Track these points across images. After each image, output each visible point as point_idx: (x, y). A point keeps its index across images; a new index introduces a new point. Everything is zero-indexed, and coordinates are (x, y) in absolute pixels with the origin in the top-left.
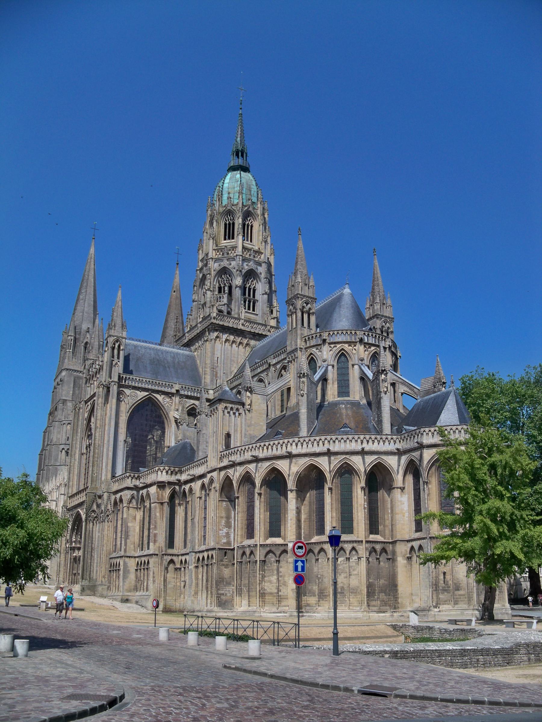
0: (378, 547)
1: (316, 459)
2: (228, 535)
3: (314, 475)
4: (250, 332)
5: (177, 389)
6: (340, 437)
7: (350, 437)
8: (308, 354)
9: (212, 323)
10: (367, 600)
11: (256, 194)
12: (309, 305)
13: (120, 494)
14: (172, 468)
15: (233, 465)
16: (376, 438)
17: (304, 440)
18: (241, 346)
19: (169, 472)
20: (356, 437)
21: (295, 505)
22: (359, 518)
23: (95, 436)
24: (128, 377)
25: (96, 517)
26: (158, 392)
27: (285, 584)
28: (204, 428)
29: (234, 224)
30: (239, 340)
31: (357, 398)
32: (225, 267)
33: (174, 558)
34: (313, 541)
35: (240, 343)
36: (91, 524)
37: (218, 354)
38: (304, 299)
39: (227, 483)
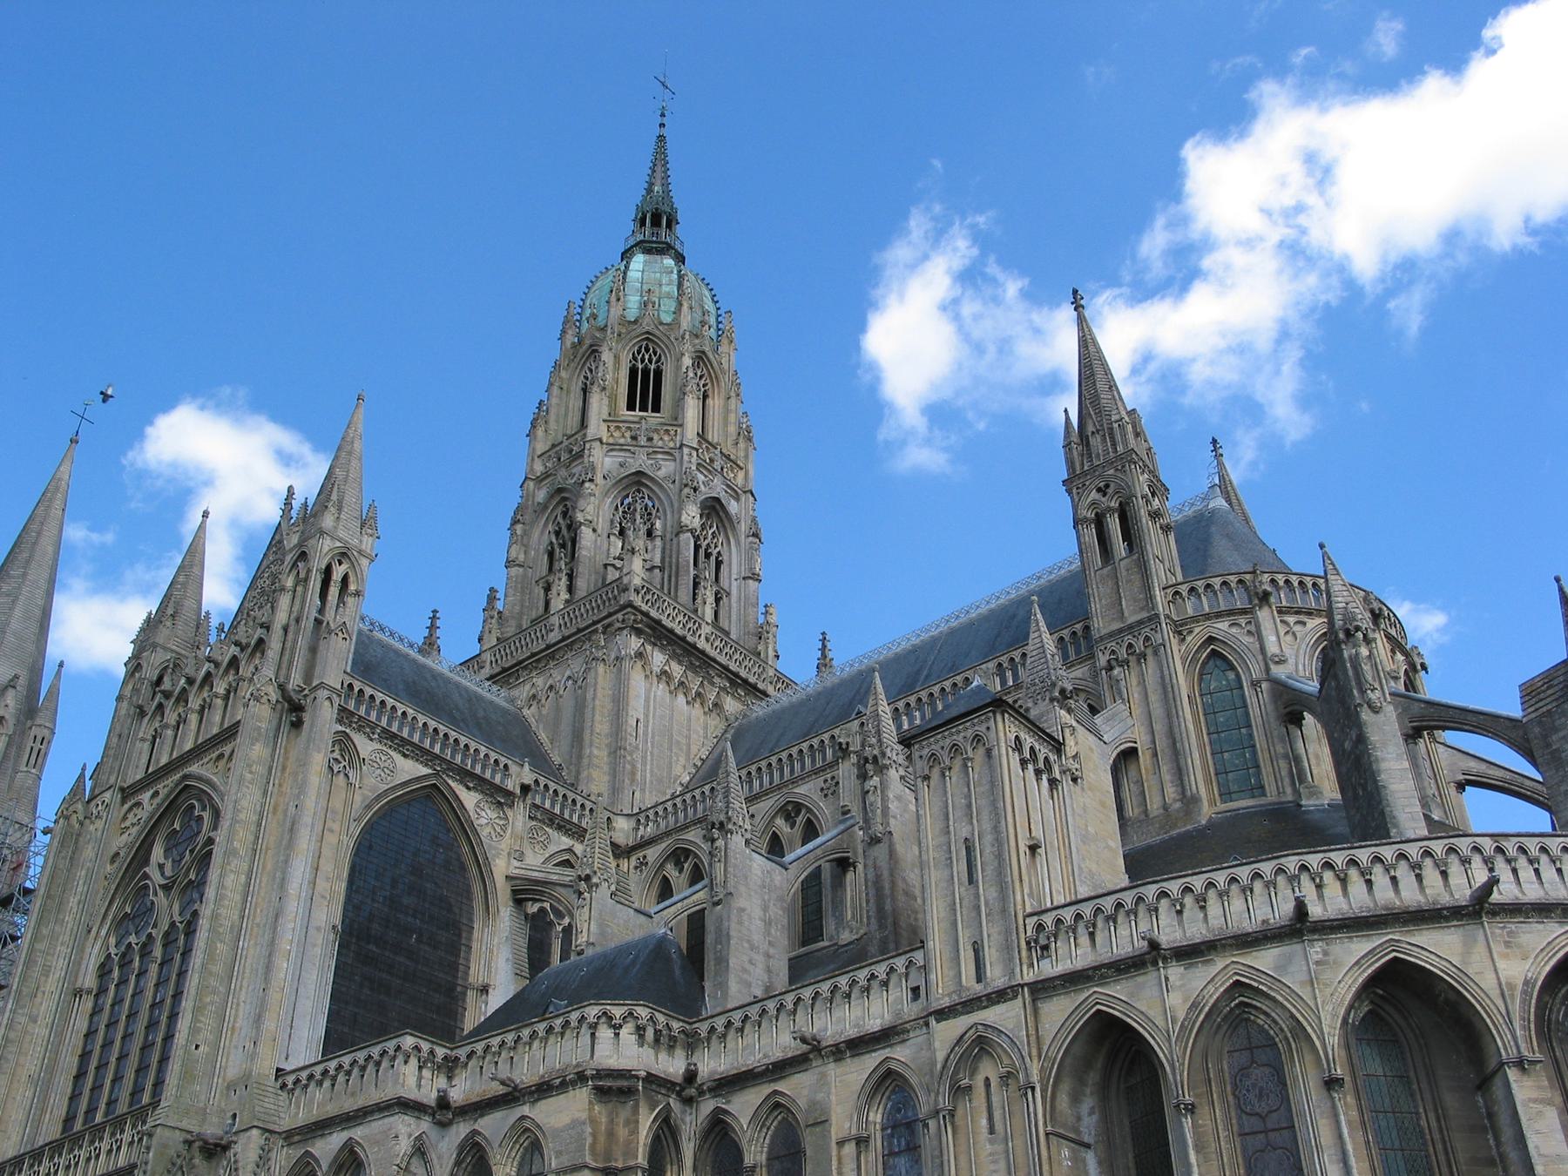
4: (726, 668)
5: (526, 782)
9: (630, 605)
13: (336, 1140)
14: (661, 1018)
15: (1152, 955)
18: (697, 705)
19: (650, 1033)
23: (221, 886)
26: (465, 776)
28: (742, 889)
29: (658, 373)
30: (695, 683)
32: (639, 473)
37: (636, 709)
39: (1114, 1050)
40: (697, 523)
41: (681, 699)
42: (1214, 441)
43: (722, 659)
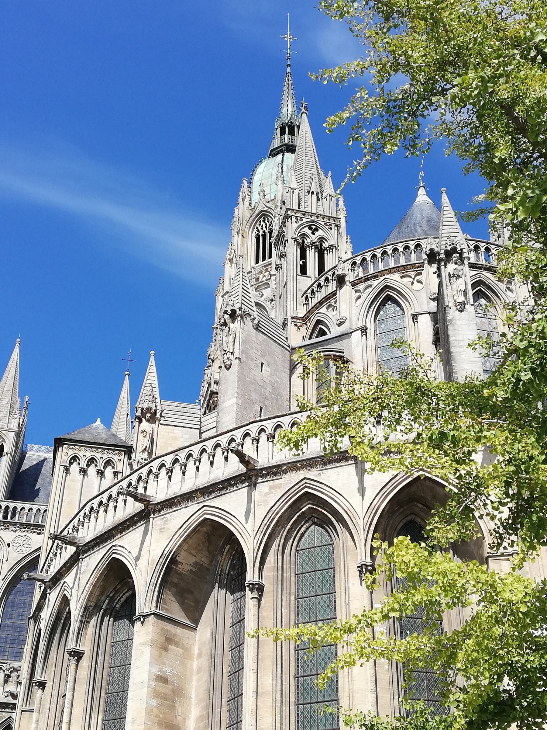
1: (217, 502)
12: (320, 233)
21: (147, 667)
24: (19, 505)
38: (305, 220)
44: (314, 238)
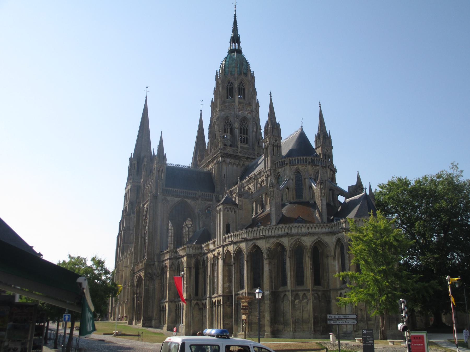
0: (320, 293)
1: (280, 239)
2: (229, 287)
3: (279, 249)
6: (294, 225)
7: (301, 225)
8: (277, 172)
10: (314, 327)
11: (246, 68)
12: (277, 142)
16: (317, 225)
17: (273, 228)
18: (239, 167)
20: (304, 225)
22: (308, 275)
25: (150, 278)
26: (188, 198)
27: (264, 317)
29: (232, 88)
30: (237, 162)
31: (308, 199)
33: (199, 302)
34: (280, 290)
35: (239, 164)
36: (148, 282)
37: (224, 172)
40: (238, 126)
41: (235, 166)
42: (320, 103)
43: (243, 155)
44: (276, 143)
